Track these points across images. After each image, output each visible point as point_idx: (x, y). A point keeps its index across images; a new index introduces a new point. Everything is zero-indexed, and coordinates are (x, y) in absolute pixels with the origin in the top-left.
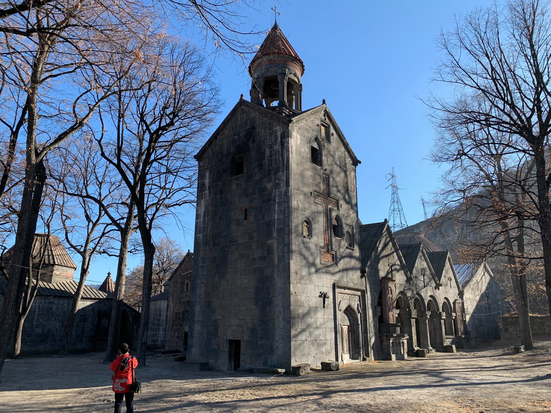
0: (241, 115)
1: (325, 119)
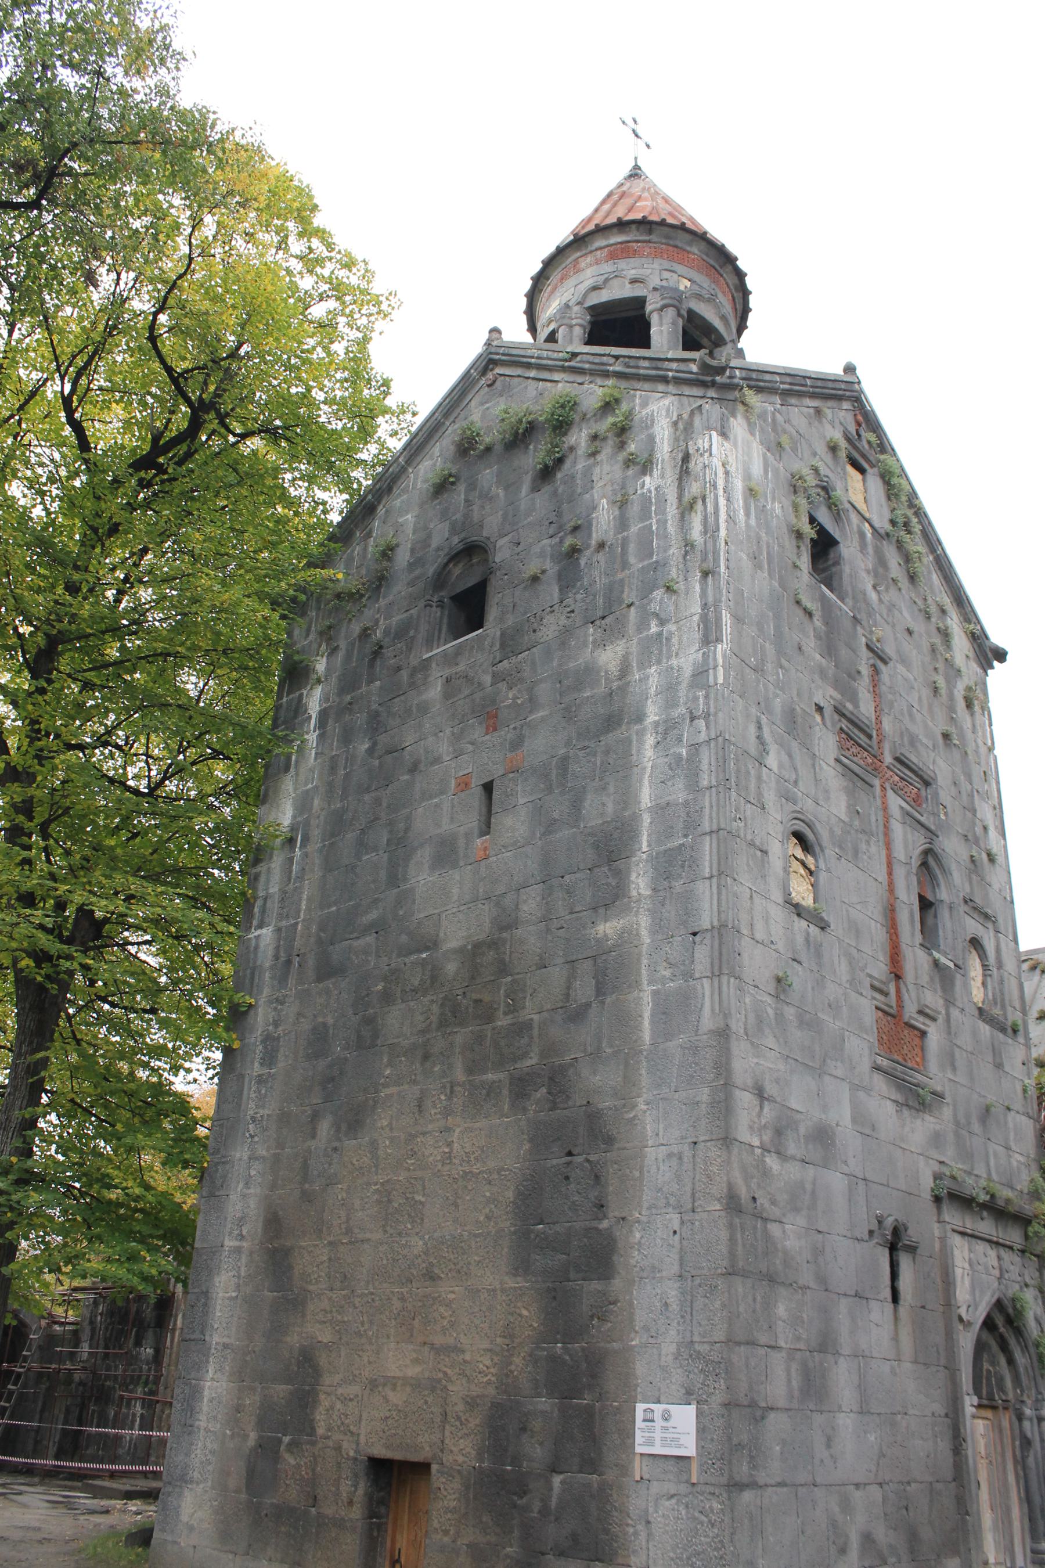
0: (483, 404)
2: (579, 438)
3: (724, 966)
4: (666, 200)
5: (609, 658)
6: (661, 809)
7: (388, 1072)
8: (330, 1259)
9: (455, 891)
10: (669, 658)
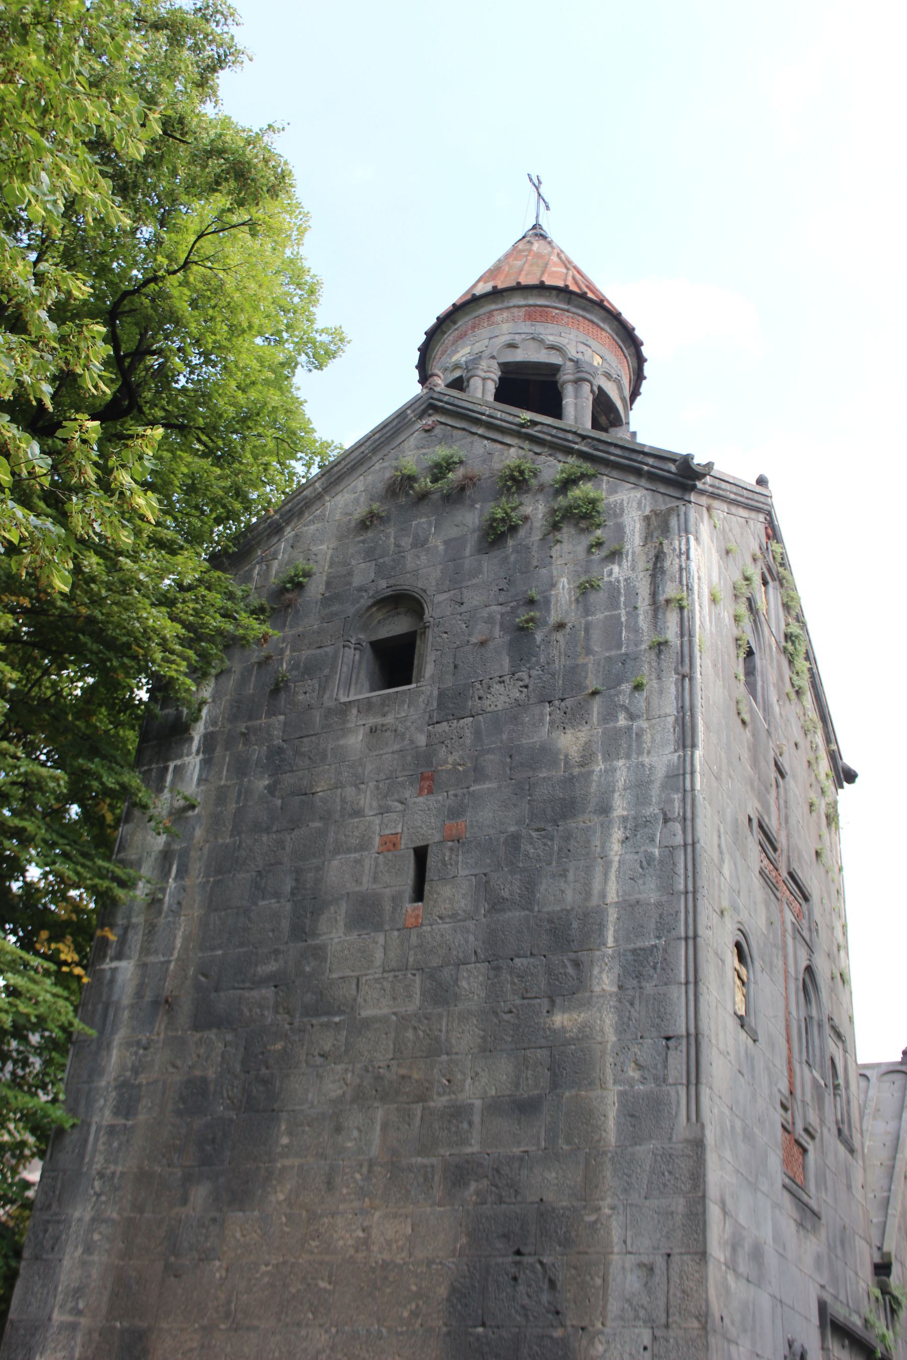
2: (536, 509)
3: (694, 1076)
4: (567, 264)
5: (570, 742)
6: (630, 907)
7: (285, 1140)
8: (203, 1346)
9: (379, 955)
10: (640, 753)
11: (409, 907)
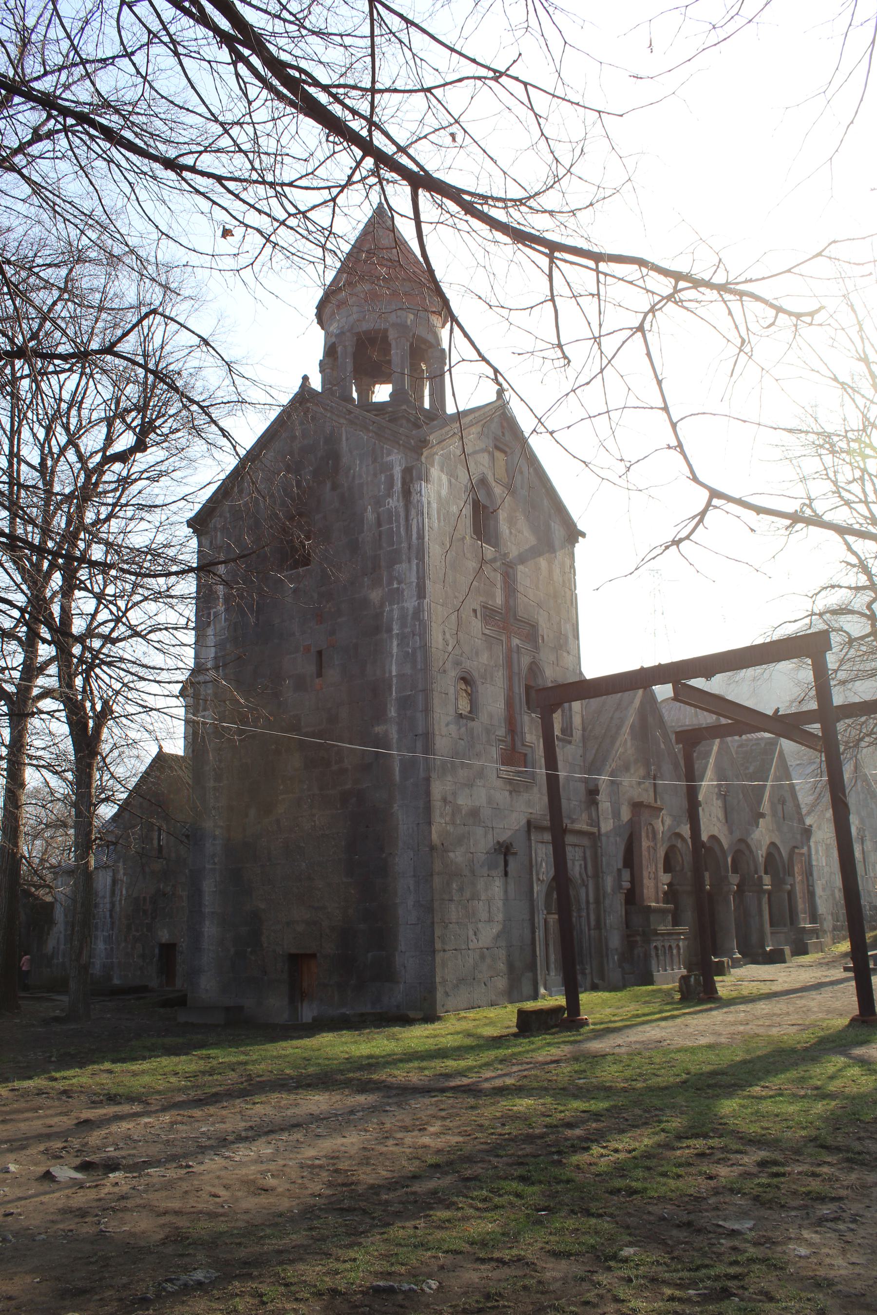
1: (503, 434)
3: (428, 748)
6: (400, 676)
11: (317, 680)
